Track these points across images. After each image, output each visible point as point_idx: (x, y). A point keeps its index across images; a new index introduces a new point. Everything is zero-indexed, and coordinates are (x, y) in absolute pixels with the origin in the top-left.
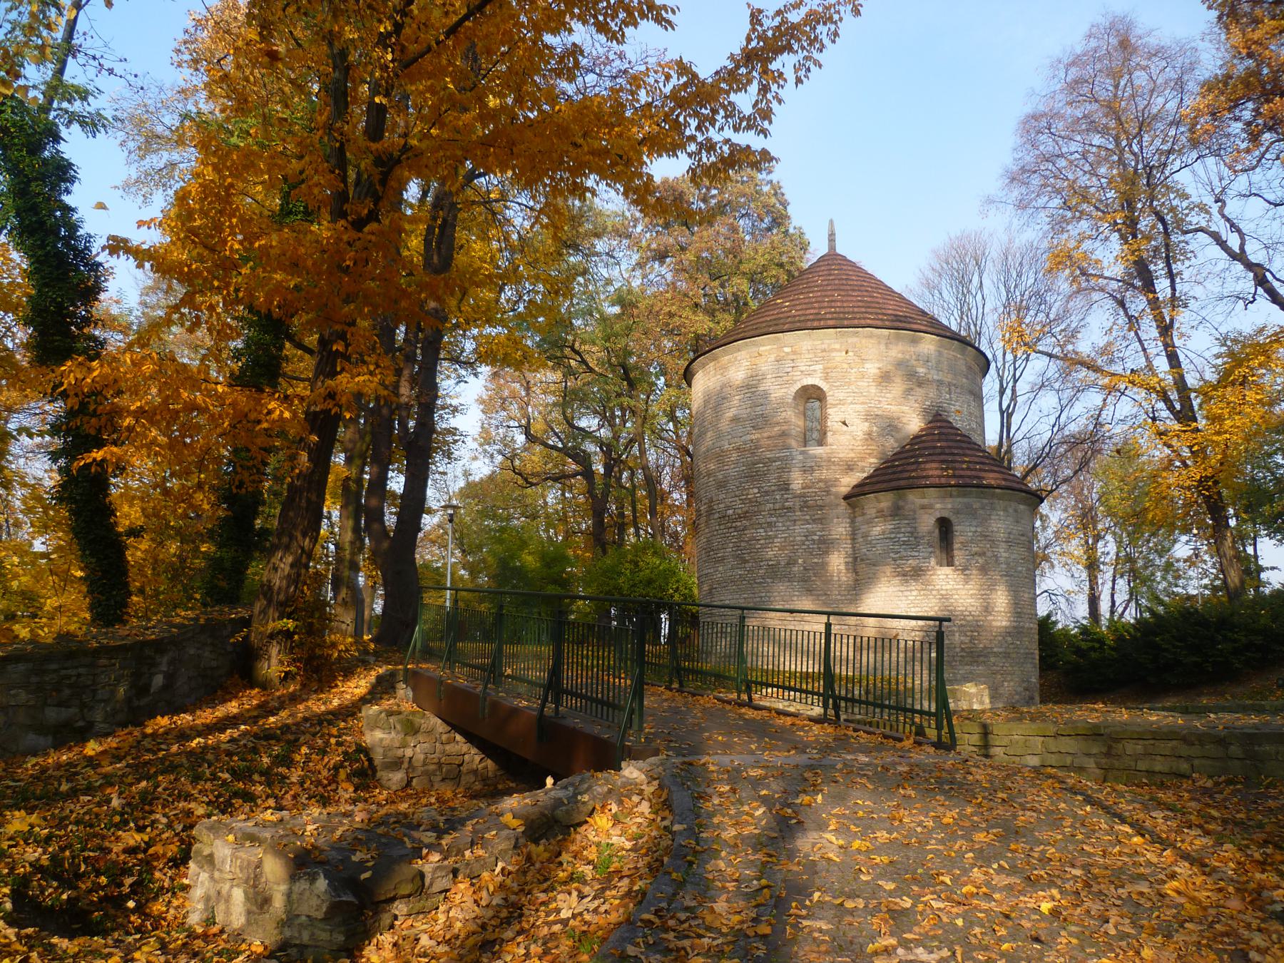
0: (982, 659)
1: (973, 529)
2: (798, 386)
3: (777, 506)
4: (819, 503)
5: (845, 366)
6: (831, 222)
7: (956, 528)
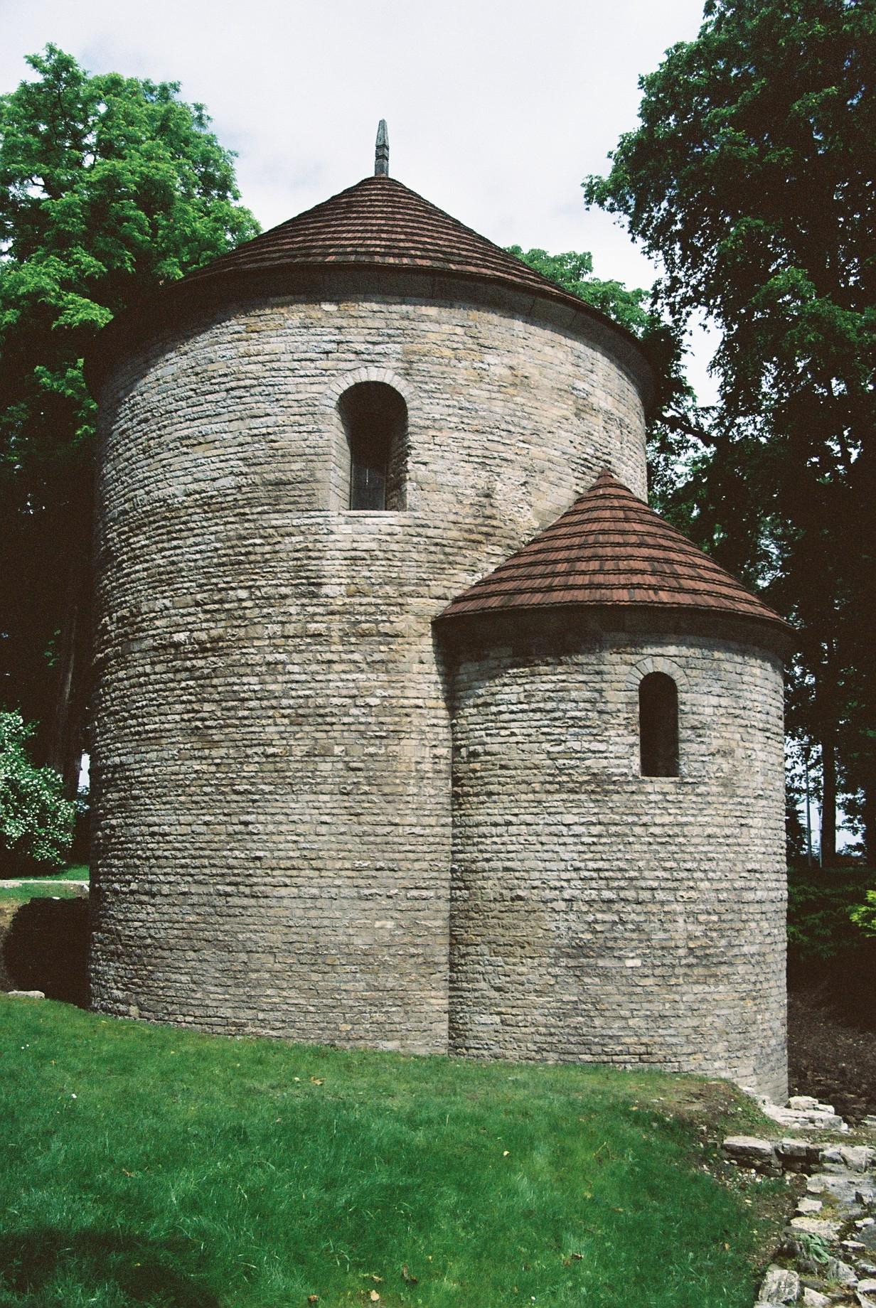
1: (715, 701)
3: (290, 630)
4: (385, 628)
5: (447, 352)
6: (382, 125)
7: (682, 696)
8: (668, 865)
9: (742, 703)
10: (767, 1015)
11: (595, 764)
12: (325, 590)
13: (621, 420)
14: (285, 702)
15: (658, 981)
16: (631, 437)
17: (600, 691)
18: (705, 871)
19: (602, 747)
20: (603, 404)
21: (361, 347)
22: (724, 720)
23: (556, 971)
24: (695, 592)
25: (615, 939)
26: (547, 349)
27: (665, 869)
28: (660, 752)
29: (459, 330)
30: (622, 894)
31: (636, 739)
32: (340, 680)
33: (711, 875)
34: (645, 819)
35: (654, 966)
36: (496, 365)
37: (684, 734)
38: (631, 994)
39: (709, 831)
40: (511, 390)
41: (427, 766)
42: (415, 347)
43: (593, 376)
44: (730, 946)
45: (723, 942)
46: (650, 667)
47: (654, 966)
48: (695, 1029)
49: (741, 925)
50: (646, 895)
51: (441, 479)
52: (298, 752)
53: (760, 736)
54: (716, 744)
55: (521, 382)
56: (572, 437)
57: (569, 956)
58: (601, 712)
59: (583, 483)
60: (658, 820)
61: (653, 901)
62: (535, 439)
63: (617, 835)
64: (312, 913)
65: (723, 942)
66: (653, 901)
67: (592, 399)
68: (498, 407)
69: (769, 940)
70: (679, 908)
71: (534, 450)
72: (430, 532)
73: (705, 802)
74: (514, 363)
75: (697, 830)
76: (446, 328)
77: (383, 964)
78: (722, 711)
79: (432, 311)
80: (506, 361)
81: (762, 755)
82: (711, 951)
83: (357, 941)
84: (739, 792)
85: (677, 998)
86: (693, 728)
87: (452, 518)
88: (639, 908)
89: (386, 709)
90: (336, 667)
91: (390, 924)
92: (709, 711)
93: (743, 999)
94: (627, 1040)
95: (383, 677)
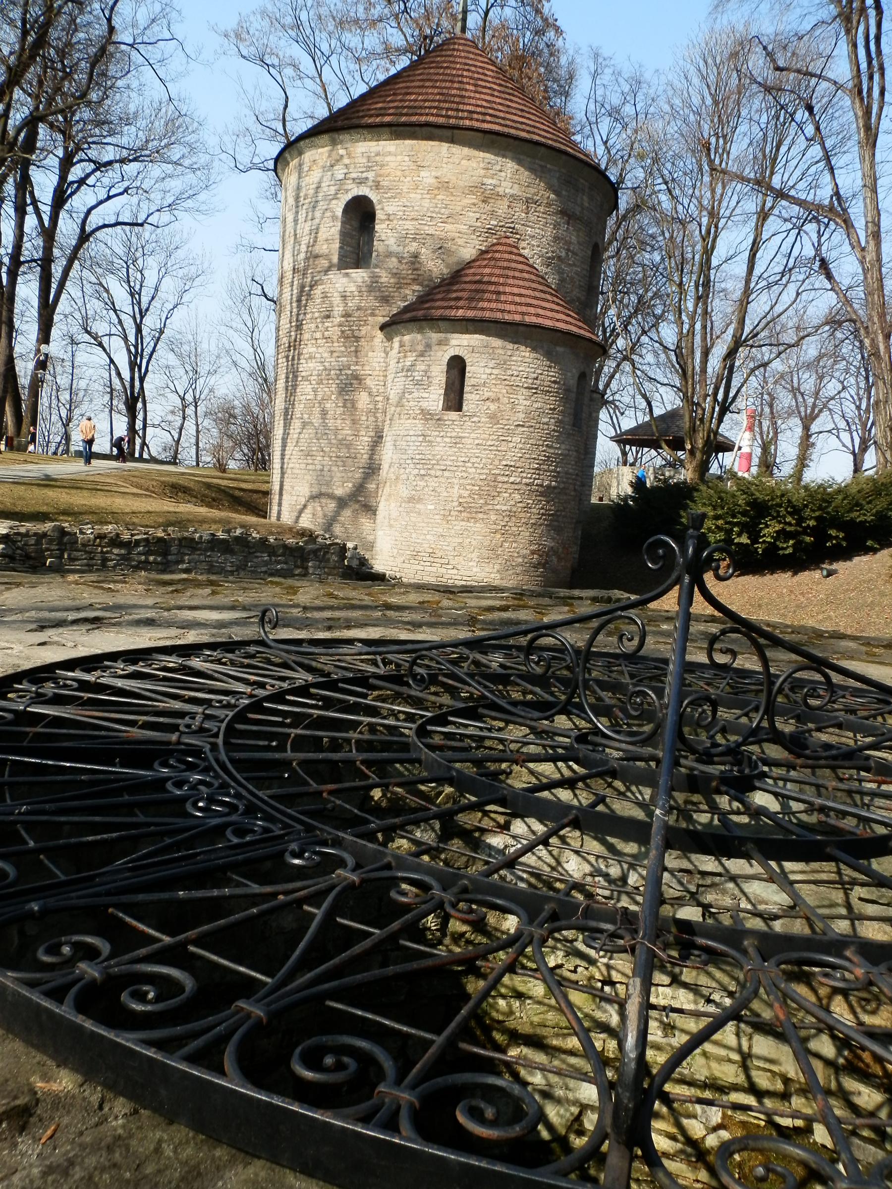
0: (481, 516)
2: (349, 196)
5: (399, 173)
9: (509, 372)
10: (514, 545)
11: (424, 405)
13: (527, 199)
16: (541, 209)
17: (429, 366)
19: (426, 395)
20: (507, 191)
24: (483, 309)
26: (464, 162)
28: (455, 397)
29: (407, 159)
31: (443, 391)
37: (466, 389)
39: (477, 442)
40: (436, 192)
42: (382, 172)
43: (503, 174)
45: (482, 501)
46: (452, 352)
54: (487, 395)
55: (443, 186)
56: (478, 215)
62: (450, 220)
65: (482, 501)
67: (497, 189)
68: (426, 203)
70: (456, 481)
71: (449, 227)
74: (439, 174)
75: (470, 441)
76: (399, 158)
80: (433, 174)
81: (525, 402)
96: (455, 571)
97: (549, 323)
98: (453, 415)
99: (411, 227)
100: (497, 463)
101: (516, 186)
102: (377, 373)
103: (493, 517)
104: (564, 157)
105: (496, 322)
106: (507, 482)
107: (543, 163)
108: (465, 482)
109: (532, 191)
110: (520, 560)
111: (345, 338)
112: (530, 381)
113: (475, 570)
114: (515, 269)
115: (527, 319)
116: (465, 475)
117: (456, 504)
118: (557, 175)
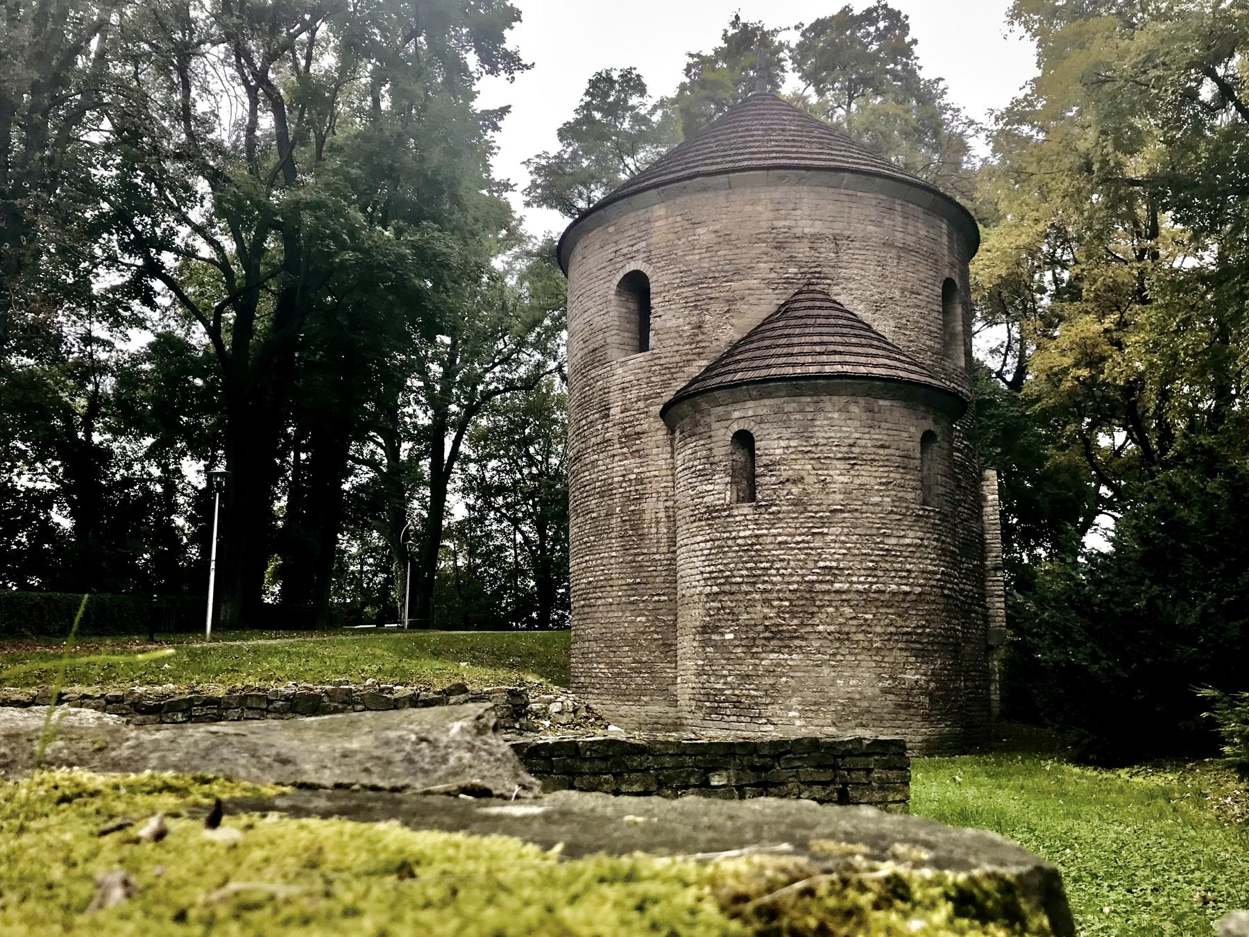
0: (797, 642)
1: (783, 443)
3: (599, 439)
4: (638, 429)
5: (672, 236)
7: (757, 444)
8: (749, 565)
12: (612, 412)
14: (598, 484)
15: (745, 649)
16: (857, 244)
17: (710, 449)
18: (778, 569)
19: (710, 487)
20: (807, 230)
21: (625, 251)
22: (793, 456)
23: (695, 644)
25: (719, 620)
26: (748, 208)
27: (747, 569)
29: (679, 219)
30: (723, 588)
32: (618, 467)
33: (782, 571)
34: (734, 534)
35: (742, 639)
36: (704, 234)
37: (759, 471)
38: (729, 659)
39: (780, 539)
40: (716, 248)
41: (662, 515)
42: (652, 240)
43: (798, 212)
44: (802, 624)
45: (795, 621)
46: (735, 427)
47: (742, 639)
48: (772, 686)
49: (815, 609)
50: (735, 588)
51: (669, 324)
52: (603, 513)
53: (841, 465)
54: (785, 475)
56: (771, 265)
57: (698, 632)
58: (712, 464)
59: (785, 297)
60: (742, 534)
61: (740, 592)
62: (736, 277)
63: (719, 547)
64: (610, 615)
66: (740, 592)
69: (855, 622)
70: (757, 596)
72: (662, 361)
73: (777, 517)
74: (718, 227)
75: (769, 539)
77: (641, 645)
78: (791, 450)
79: (662, 212)
80: (711, 228)
81: (842, 479)
82: (785, 628)
83: (629, 630)
84: (809, 508)
85: (757, 662)
86: (765, 466)
87: (676, 348)
88: (732, 597)
89: (640, 481)
90: (617, 458)
91: (643, 619)
92: (779, 451)
93: (817, 666)
94: (727, 692)
95: (638, 460)
96: (772, 727)
97: (863, 370)
98: (746, 509)
99: (690, 294)
100: (811, 565)
101: (818, 222)
102: (664, 473)
103: (816, 644)
104: (878, 180)
105: (783, 379)
106: (828, 592)
107: (850, 192)
108: (770, 596)
109: (841, 225)
110: (865, 704)
111: (626, 437)
112: (845, 449)
113: (798, 723)
114: (818, 316)
115: (827, 369)
116: (769, 587)
117: (760, 628)
118: (874, 202)
